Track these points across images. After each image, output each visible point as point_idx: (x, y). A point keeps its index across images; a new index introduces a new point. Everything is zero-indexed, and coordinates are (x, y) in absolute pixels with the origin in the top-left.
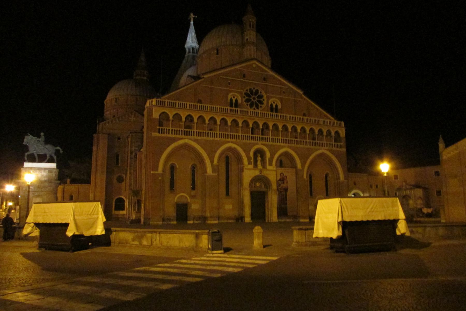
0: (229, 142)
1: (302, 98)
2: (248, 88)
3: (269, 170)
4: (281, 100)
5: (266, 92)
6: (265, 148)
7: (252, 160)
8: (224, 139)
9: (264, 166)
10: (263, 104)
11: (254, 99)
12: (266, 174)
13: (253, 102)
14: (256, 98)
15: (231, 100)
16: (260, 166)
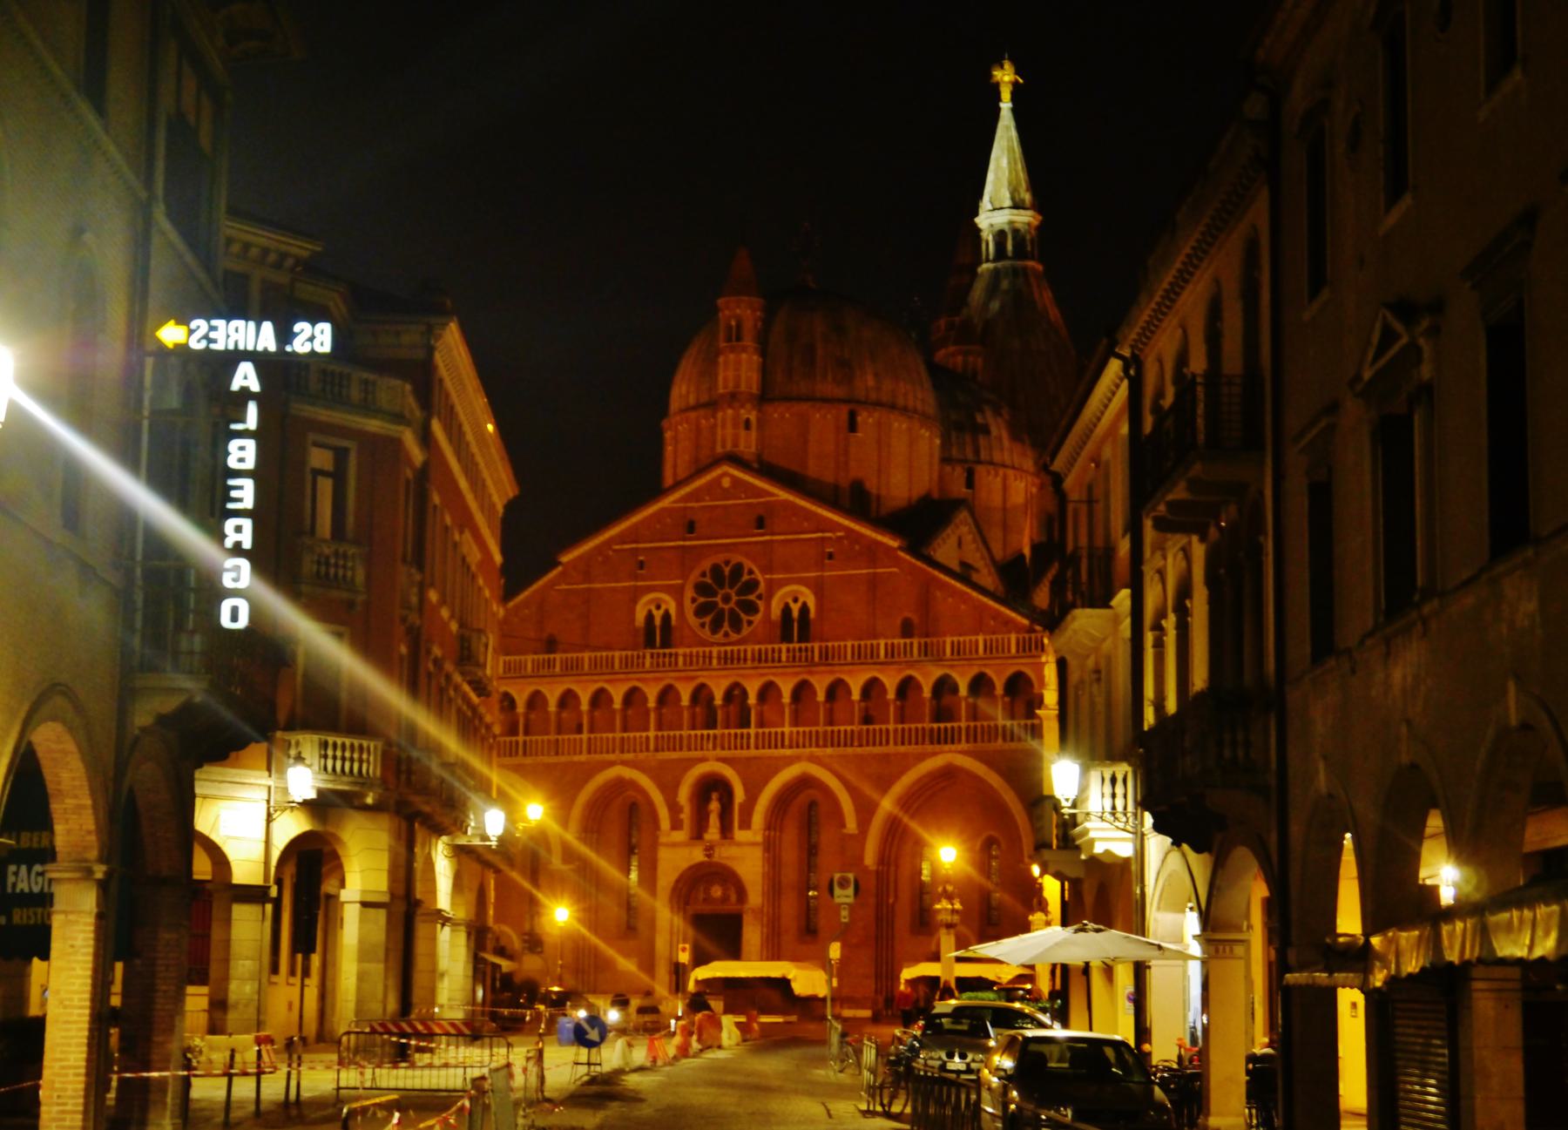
0: (611, 764)
1: (897, 562)
2: (706, 565)
3: (739, 844)
4: (818, 588)
5: (764, 571)
6: (729, 773)
7: (686, 816)
8: (598, 757)
9: (726, 830)
10: (756, 610)
11: (727, 599)
12: (728, 858)
13: (723, 610)
14: (733, 594)
15: (650, 617)
16: (713, 833)
